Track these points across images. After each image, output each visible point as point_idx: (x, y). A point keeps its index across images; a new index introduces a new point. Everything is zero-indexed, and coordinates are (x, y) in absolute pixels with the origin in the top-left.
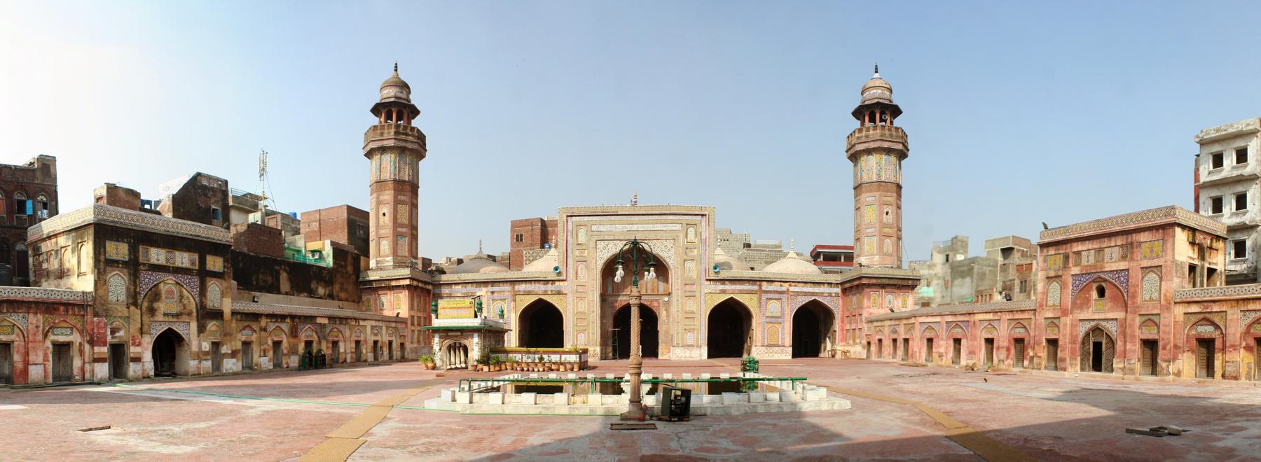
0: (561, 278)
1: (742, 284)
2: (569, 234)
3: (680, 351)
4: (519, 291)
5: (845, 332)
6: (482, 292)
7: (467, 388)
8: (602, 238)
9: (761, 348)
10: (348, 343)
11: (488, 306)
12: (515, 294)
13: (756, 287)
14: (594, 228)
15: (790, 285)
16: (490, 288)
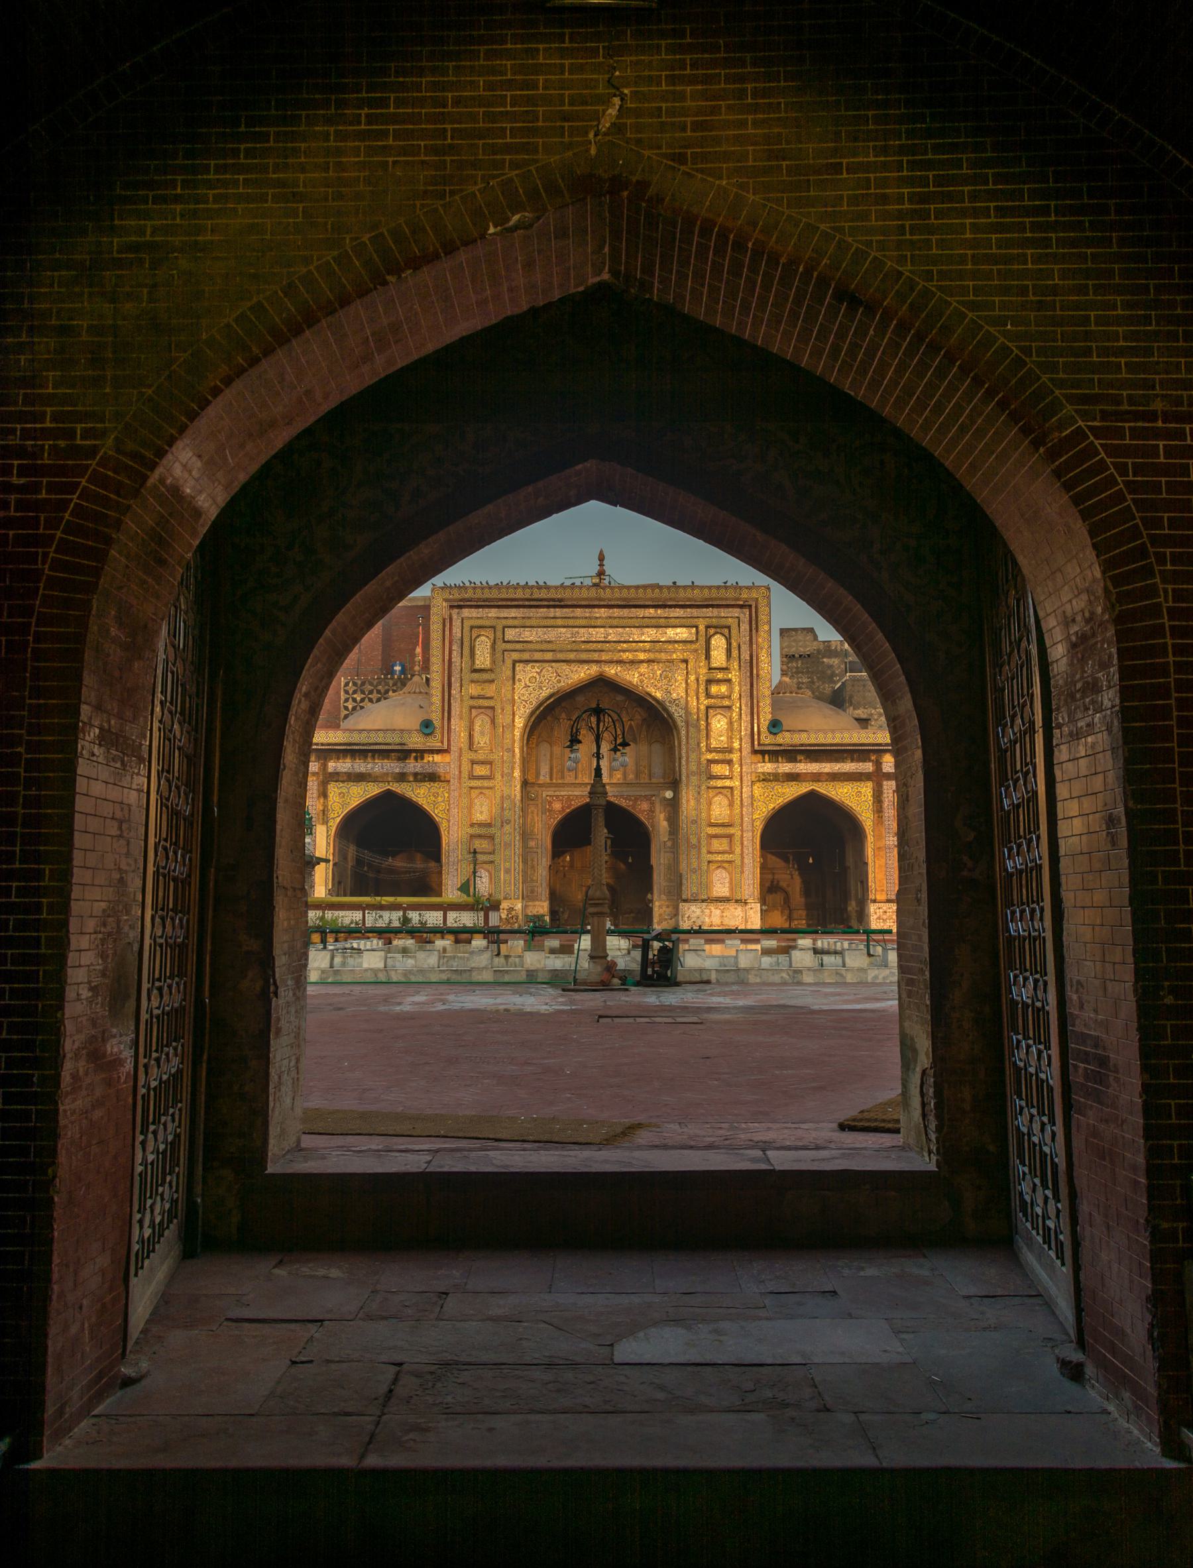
0: (438, 745)
1: (837, 761)
3: (698, 912)
4: (338, 774)
13: (868, 767)
14: (510, 634)
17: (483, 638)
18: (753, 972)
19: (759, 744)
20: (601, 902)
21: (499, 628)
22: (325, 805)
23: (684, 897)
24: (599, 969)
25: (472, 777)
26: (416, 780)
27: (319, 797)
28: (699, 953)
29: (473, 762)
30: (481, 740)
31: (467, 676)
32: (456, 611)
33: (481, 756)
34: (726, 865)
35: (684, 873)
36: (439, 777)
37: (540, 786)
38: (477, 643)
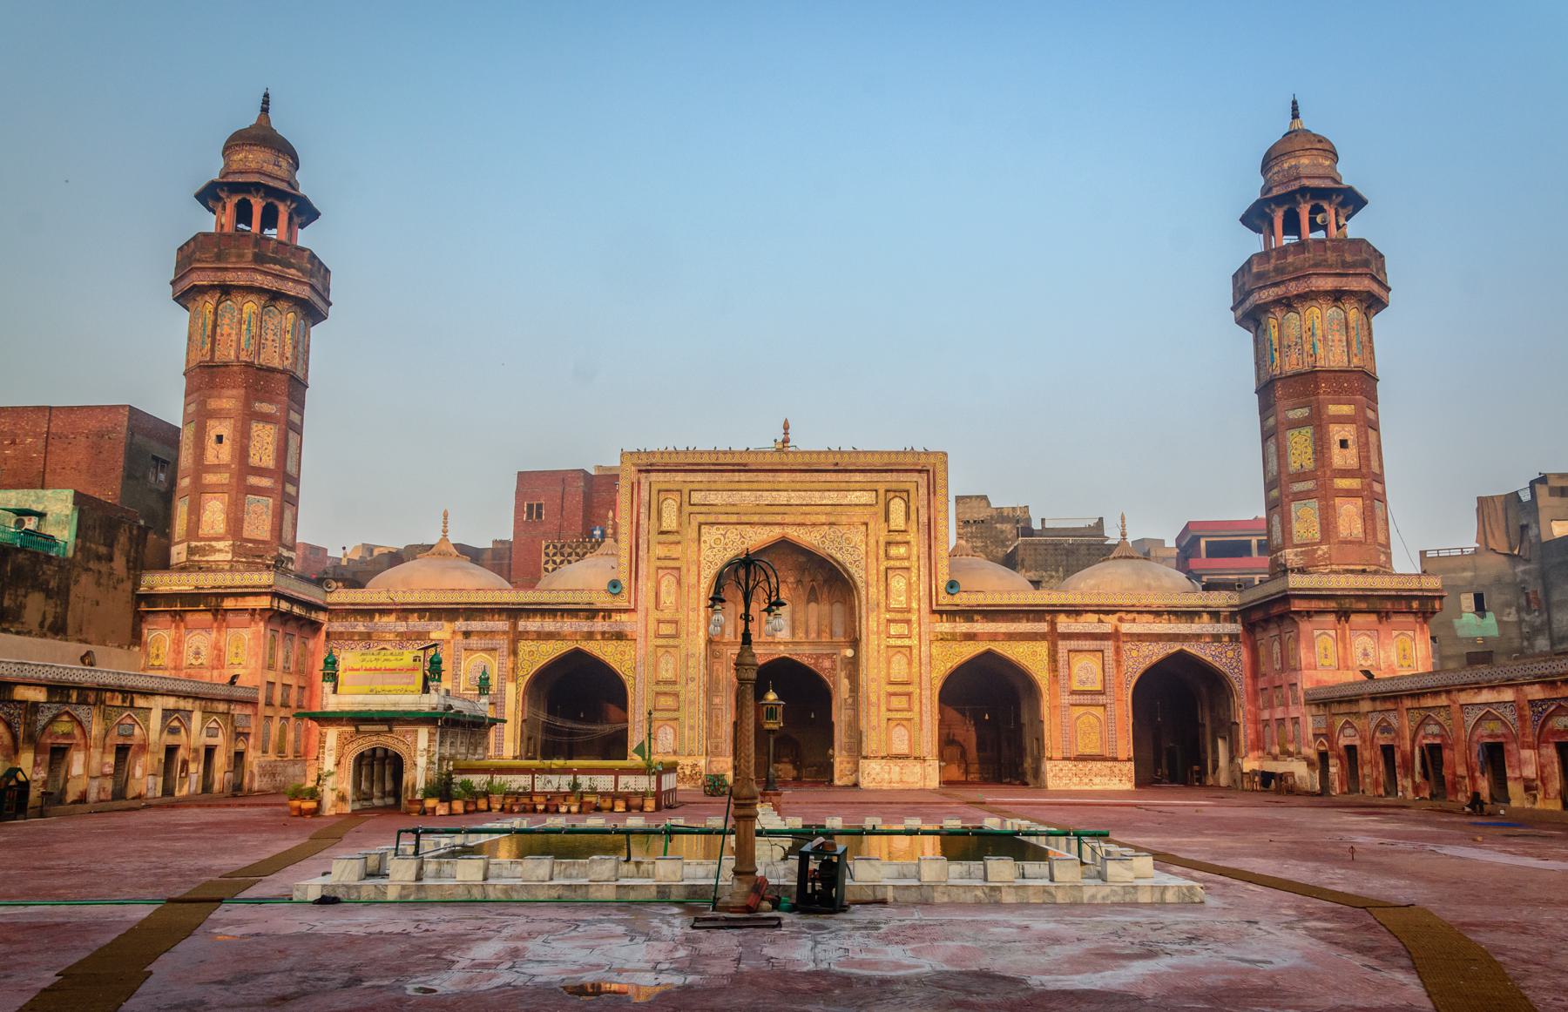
0: (625, 605)
1: (1013, 621)
2: (642, 510)
3: (878, 768)
4: (527, 632)
5: (1260, 727)
6: (441, 631)
7: (411, 850)
8: (711, 519)
9: (1061, 764)
10: (96, 754)
11: (456, 664)
12: (517, 637)
13: (1043, 627)
15: (1121, 620)
16: (461, 625)
17: (670, 501)
18: (939, 889)
19: (937, 605)
20: (748, 802)
21: (686, 492)
22: (515, 664)
23: (864, 754)
24: (745, 888)
25: (658, 636)
26: (603, 639)
27: (509, 655)
28: (873, 862)
29: (659, 622)
30: (668, 599)
31: (654, 537)
32: (644, 474)
33: (667, 615)
34: (905, 723)
35: (864, 730)
36: (626, 636)
37: (726, 644)
38: (664, 506)
